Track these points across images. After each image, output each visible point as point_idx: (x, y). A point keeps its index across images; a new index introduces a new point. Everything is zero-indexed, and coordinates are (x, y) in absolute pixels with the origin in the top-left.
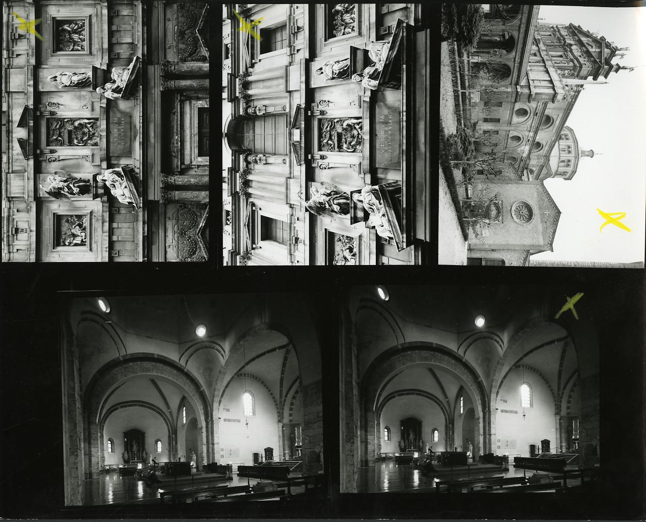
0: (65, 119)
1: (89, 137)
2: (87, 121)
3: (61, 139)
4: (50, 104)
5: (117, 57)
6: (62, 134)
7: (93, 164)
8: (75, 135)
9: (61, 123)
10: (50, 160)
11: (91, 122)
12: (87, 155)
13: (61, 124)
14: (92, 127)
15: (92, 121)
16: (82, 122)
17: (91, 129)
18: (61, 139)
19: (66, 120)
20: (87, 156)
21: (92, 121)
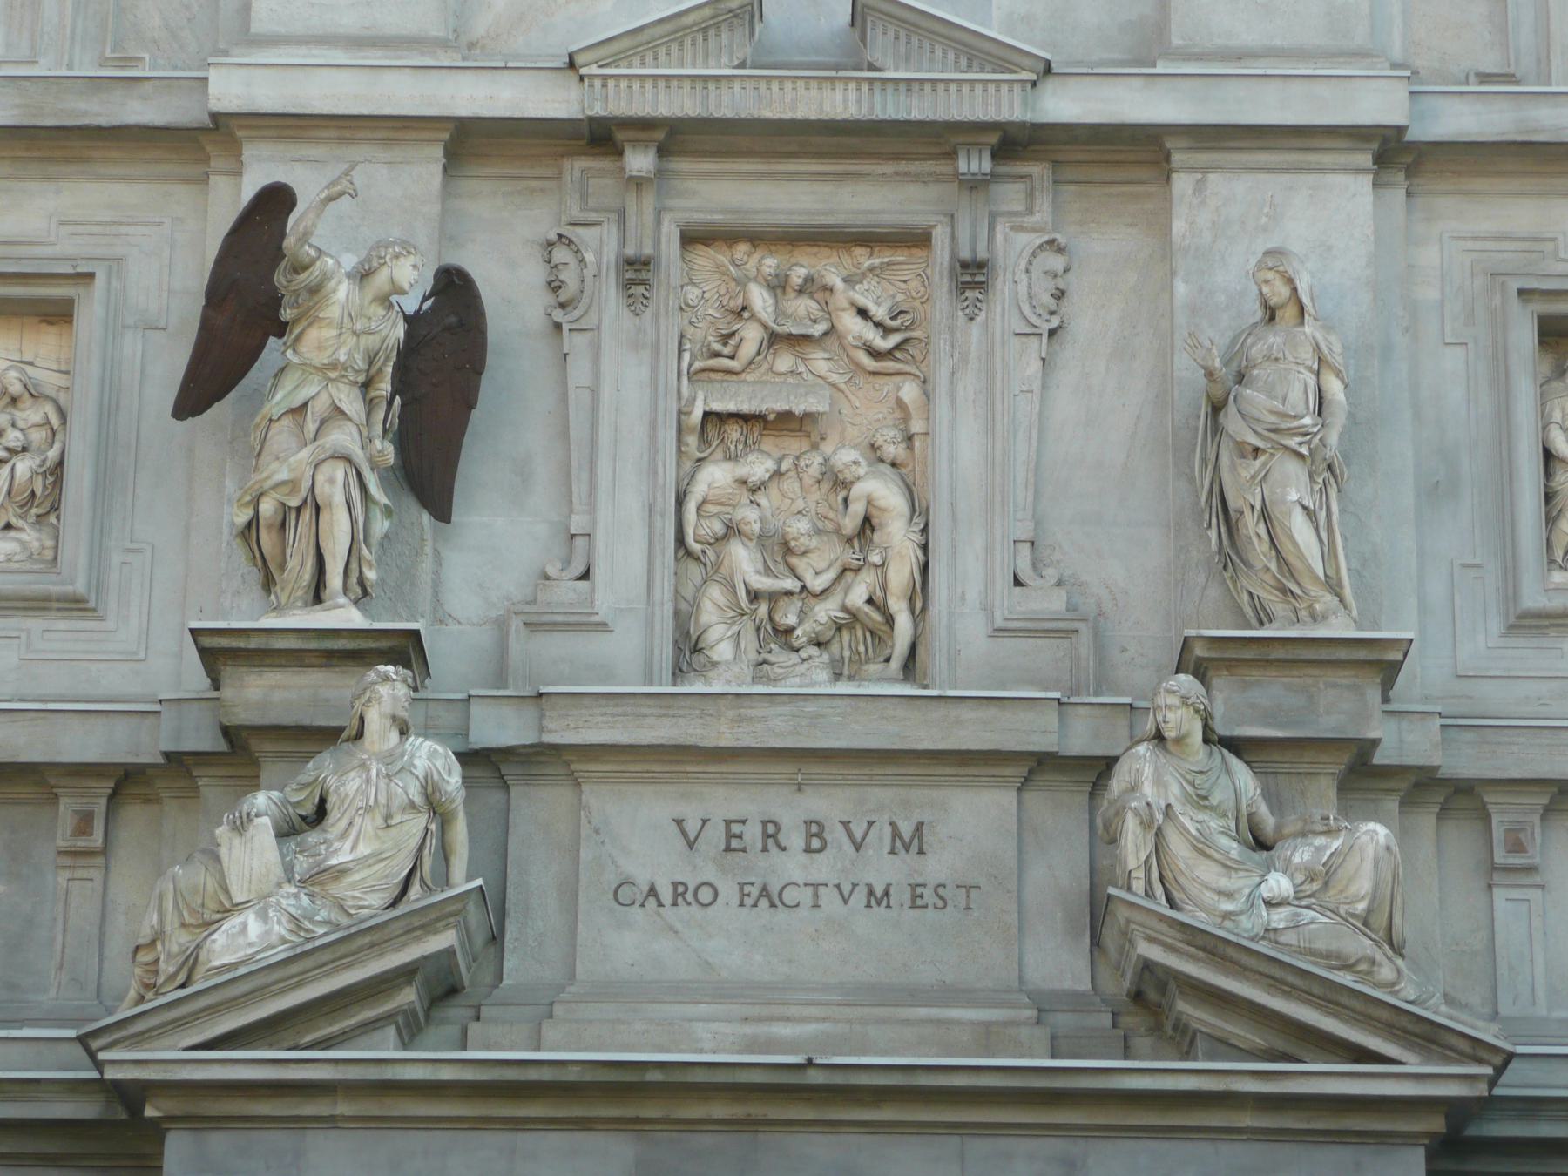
0: (927, 396)
1: (754, 596)
2: (900, 574)
3: (748, 350)
4: (1057, 262)
5: (1500, 857)
6: (784, 362)
7: (516, 623)
8: (777, 474)
9: (888, 354)
10: (561, 254)
11: (890, 620)
12: (599, 573)
13: (875, 354)
14: (850, 620)
15: (903, 623)
16: (898, 535)
17: (826, 611)
18: (748, 350)
19: (909, 392)
20: (585, 576)
21: (903, 623)
